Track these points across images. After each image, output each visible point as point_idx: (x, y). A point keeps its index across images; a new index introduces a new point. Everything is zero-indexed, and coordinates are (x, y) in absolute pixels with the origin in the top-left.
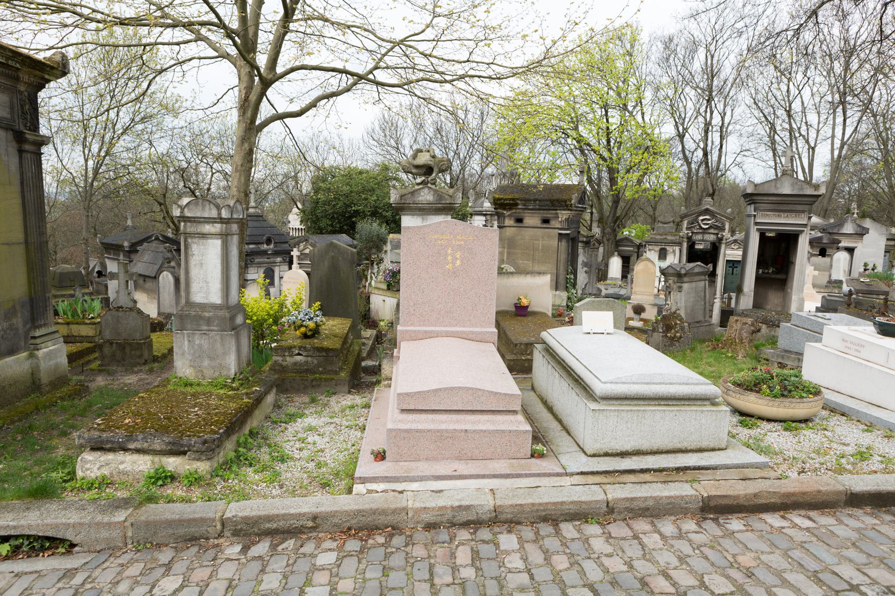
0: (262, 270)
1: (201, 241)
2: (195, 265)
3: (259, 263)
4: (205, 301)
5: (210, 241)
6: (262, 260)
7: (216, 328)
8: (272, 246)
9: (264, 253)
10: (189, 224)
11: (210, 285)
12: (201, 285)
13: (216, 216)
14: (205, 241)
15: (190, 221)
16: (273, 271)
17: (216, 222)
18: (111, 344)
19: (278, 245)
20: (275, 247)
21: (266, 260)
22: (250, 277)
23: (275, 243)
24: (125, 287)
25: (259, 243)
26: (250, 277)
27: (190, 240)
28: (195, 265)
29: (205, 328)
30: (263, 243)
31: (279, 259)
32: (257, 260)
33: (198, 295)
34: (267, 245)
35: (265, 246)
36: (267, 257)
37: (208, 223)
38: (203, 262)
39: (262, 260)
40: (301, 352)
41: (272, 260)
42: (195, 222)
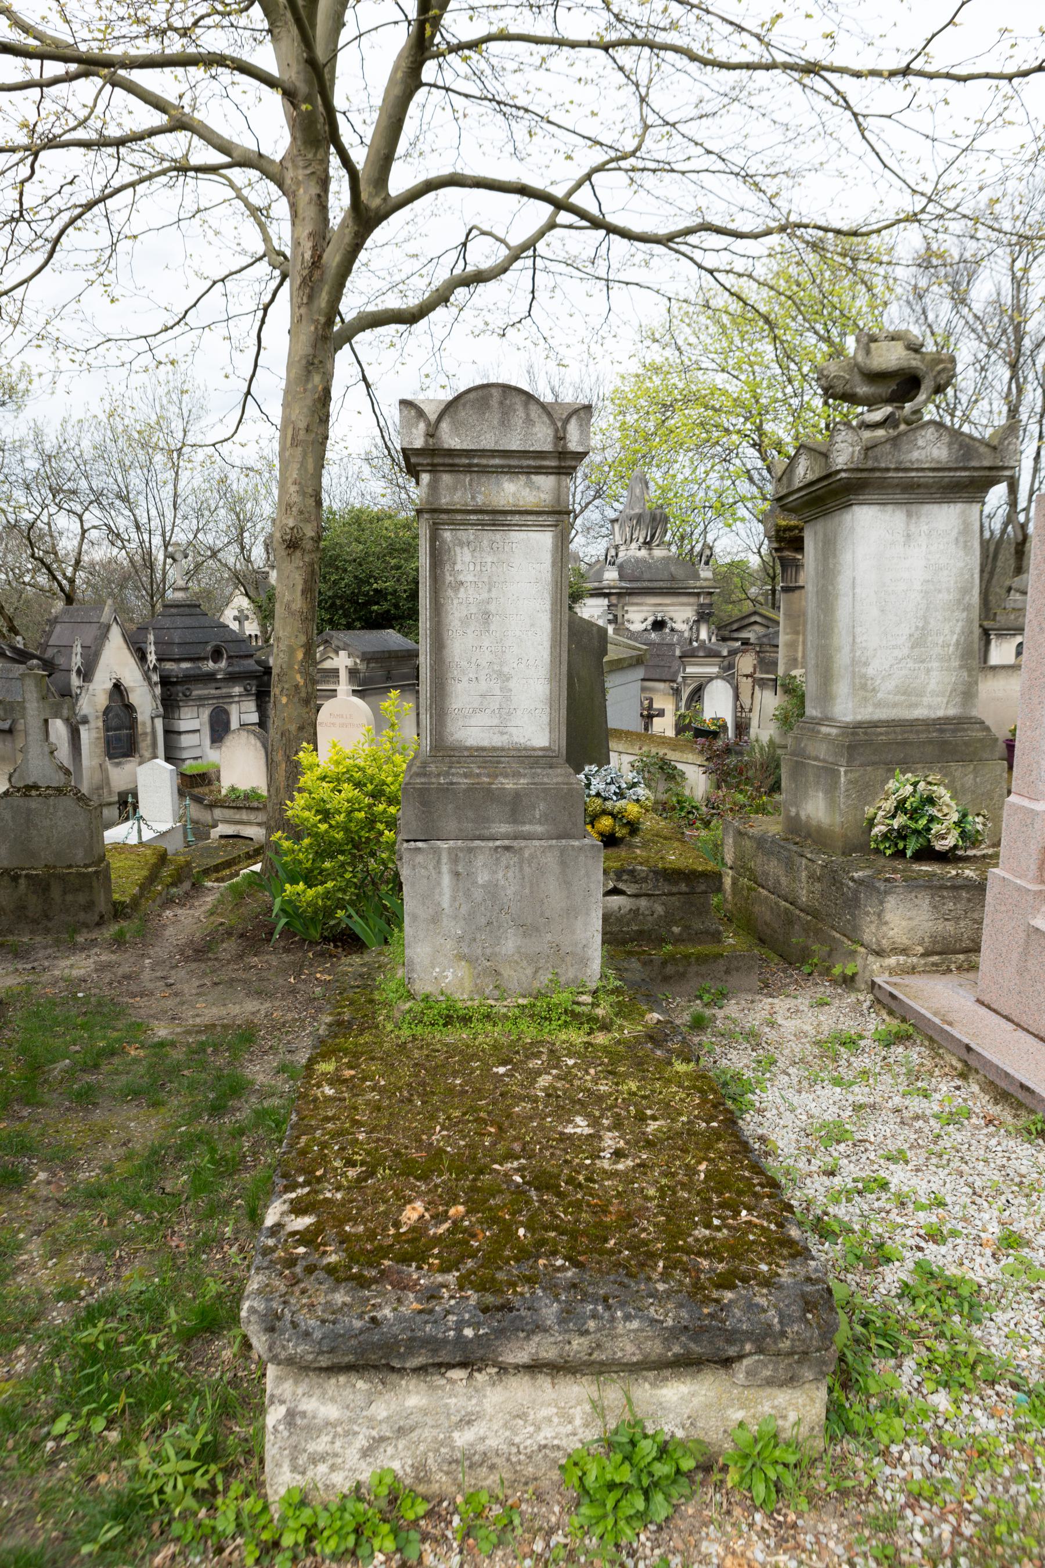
0: (206, 714)
1: (487, 537)
2: (465, 621)
3: (200, 698)
4: (497, 741)
5: (517, 536)
6: (206, 692)
7: (539, 829)
8: (223, 664)
9: (209, 678)
10: (446, 478)
11: (511, 684)
12: (483, 686)
13: (548, 447)
14: (498, 536)
15: (453, 469)
16: (227, 713)
17: (539, 471)
18: (15, 878)
19: (235, 661)
20: (229, 665)
21: (213, 692)
22: (184, 725)
23: (229, 657)
24: (42, 737)
25: (199, 659)
26: (184, 725)
27: (447, 535)
28: (465, 621)
29: (504, 828)
30: (206, 659)
31: (237, 690)
32: (196, 693)
33: (473, 721)
34: (215, 662)
35: (211, 664)
36: (214, 685)
37: (512, 471)
38: (492, 608)
39: (206, 692)
40: (621, 886)
41: (224, 690)
42: (468, 469)
